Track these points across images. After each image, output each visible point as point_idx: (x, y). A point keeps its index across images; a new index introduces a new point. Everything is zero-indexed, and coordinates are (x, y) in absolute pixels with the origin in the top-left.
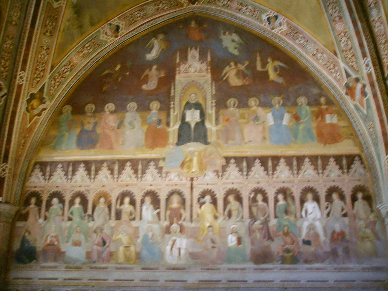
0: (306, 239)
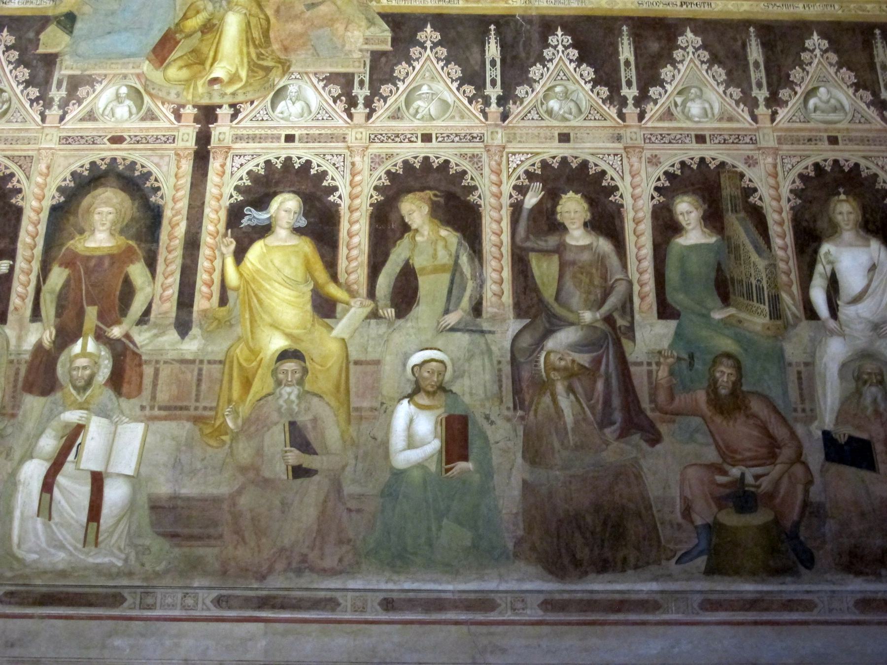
0: (843, 433)
